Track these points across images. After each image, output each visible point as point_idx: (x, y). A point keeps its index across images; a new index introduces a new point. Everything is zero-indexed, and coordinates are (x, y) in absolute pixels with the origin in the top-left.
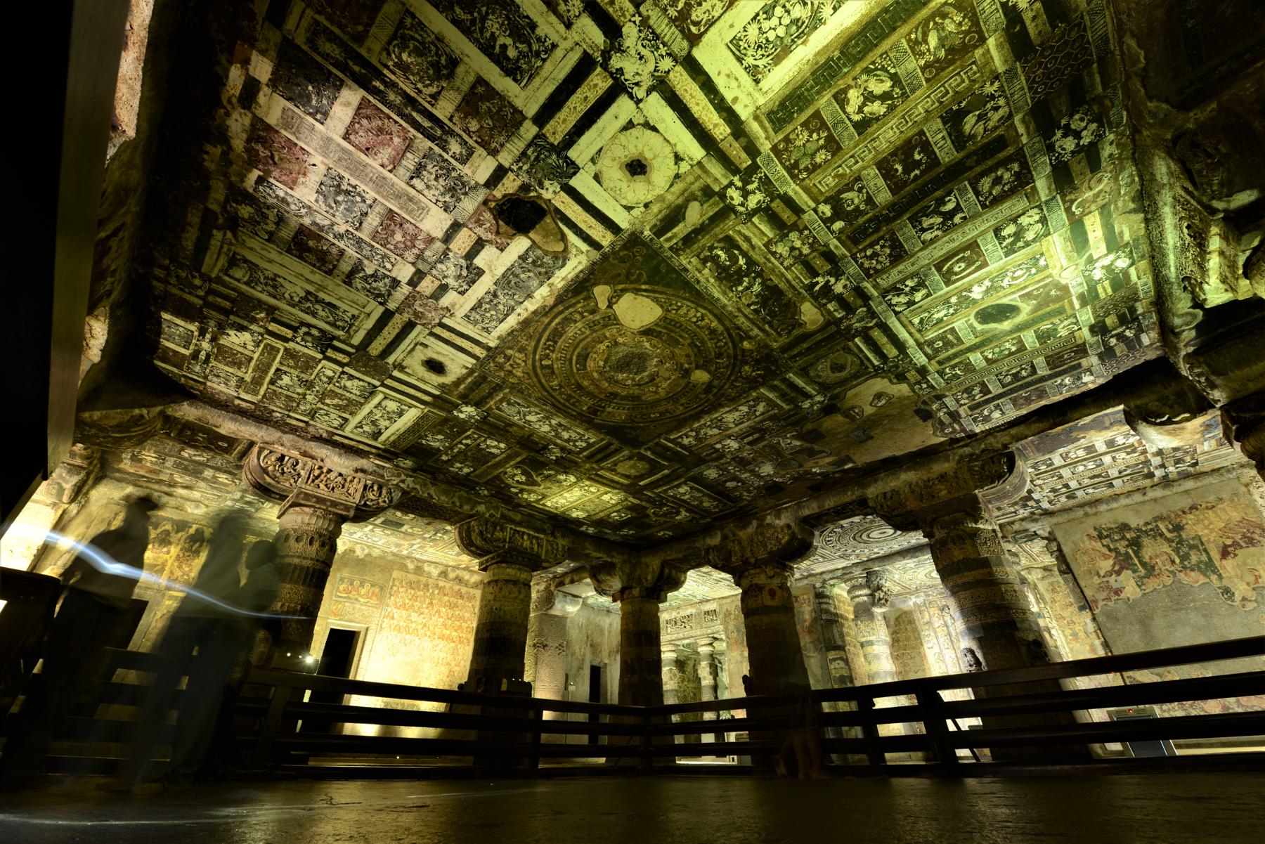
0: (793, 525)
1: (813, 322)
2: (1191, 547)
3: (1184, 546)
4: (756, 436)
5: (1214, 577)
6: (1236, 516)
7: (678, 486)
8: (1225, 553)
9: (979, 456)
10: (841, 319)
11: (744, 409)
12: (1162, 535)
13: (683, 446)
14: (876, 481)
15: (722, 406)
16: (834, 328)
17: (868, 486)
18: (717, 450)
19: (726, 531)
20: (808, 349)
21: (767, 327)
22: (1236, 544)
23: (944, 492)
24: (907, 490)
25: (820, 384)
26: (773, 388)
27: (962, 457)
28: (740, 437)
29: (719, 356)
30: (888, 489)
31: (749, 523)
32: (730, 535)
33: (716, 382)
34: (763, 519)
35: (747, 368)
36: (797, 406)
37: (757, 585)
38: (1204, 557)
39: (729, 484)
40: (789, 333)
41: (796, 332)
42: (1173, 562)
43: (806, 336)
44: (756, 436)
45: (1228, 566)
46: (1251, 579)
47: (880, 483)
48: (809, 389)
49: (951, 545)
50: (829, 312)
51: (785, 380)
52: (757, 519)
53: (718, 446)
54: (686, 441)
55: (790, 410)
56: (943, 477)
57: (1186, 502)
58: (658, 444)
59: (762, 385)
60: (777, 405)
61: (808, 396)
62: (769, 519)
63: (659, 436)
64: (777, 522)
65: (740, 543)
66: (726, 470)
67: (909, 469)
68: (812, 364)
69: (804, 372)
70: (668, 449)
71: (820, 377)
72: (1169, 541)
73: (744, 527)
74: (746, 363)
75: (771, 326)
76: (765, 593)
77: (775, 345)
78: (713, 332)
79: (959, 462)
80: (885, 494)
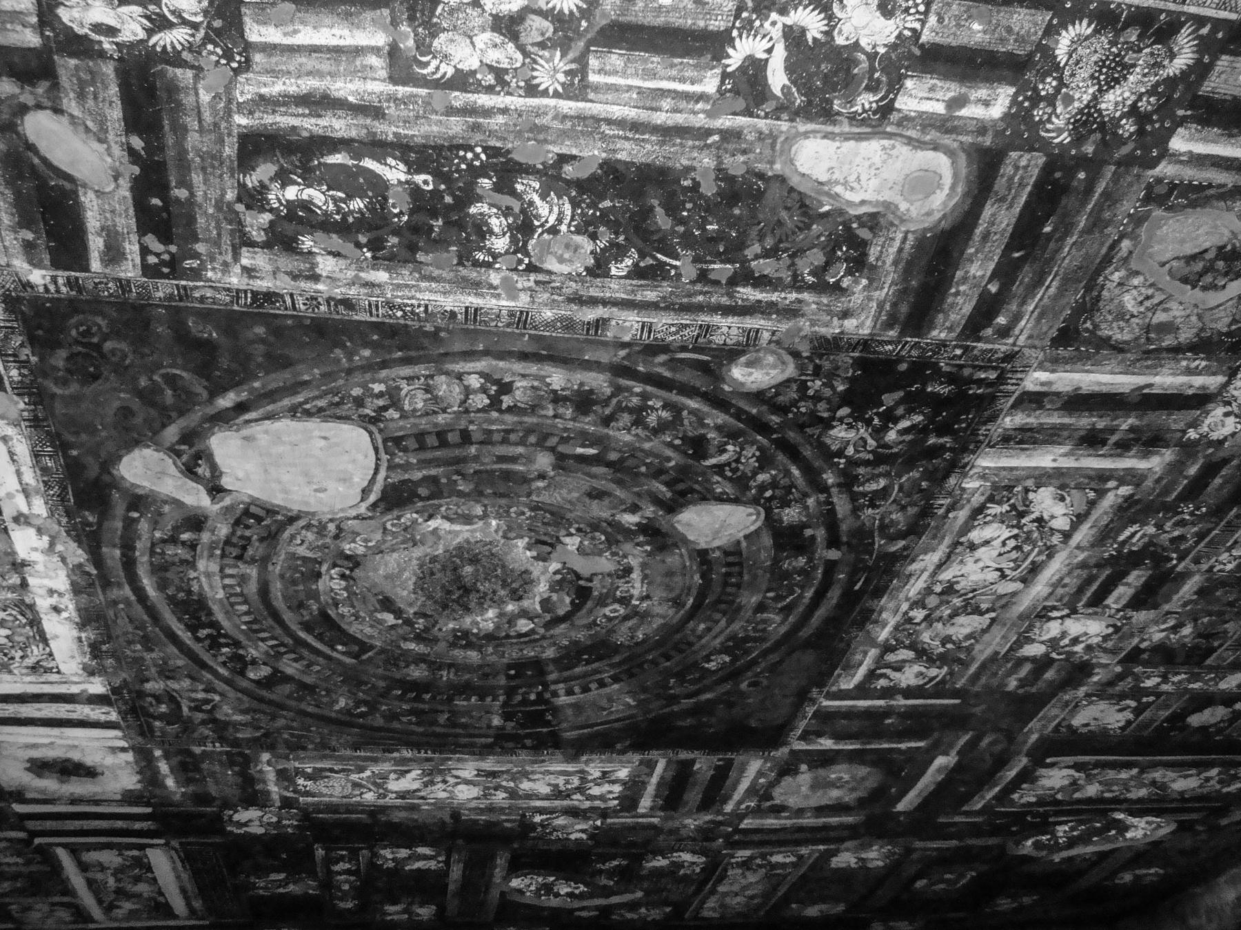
1: (921, 183)
4: (1136, 578)
7: (1026, 776)
10: (1019, 117)
11: (994, 532)
13: (909, 693)
15: (906, 556)
16: (1024, 167)
18: (1043, 663)
20: (1006, 272)
21: (748, 293)
25: (1203, 346)
26: (1025, 438)
28: (1090, 593)
29: (698, 447)
33: (791, 515)
35: (840, 433)
36: (1188, 449)
39: (1195, 720)
40: (859, 264)
41: (886, 251)
43: (939, 253)
44: (1136, 578)
48: (1166, 380)
50: (945, 125)
51: (1035, 400)
53: (1034, 650)
54: (908, 677)
55: (1175, 468)
58: (825, 717)
59: (969, 444)
60: (1103, 476)
61: (1202, 400)
63: (802, 697)
66: (1137, 692)
68: (1089, 307)
69: (1072, 340)
70: (868, 714)
71: (1168, 328)
74: (827, 424)
75: (761, 282)
77: (860, 326)
78: (584, 402)
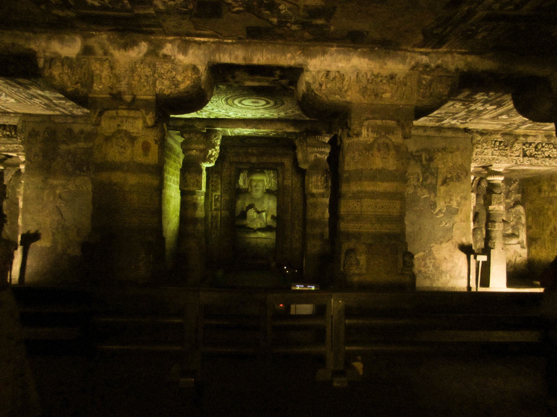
0: (202, 68)
2: (432, 174)
3: (428, 170)
5: (433, 195)
6: (460, 161)
8: (444, 182)
9: (433, 70)
12: (421, 161)
14: (324, 53)
17: (312, 55)
19: (92, 42)
22: (451, 179)
23: (388, 95)
24: (353, 77)
27: (417, 65)
30: (333, 68)
31: (134, 44)
32: (99, 52)
34: (160, 46)
37: (127, 133)
38: (434, 182)
42: (418, 180)
45: (442, 189)
46: (448, 200)
47: (328, 58)
49: (375, 152)
52: (150, 42)
56: (392, 77)
57: (442, 144)
62: (168, 49)
64: (181, 57)
65: (112, 68)
67: (363, 55)
72: (423, 166)
73: (125, 47)
76: (138, 145)
79: (413, 68)
80: (328, 72)
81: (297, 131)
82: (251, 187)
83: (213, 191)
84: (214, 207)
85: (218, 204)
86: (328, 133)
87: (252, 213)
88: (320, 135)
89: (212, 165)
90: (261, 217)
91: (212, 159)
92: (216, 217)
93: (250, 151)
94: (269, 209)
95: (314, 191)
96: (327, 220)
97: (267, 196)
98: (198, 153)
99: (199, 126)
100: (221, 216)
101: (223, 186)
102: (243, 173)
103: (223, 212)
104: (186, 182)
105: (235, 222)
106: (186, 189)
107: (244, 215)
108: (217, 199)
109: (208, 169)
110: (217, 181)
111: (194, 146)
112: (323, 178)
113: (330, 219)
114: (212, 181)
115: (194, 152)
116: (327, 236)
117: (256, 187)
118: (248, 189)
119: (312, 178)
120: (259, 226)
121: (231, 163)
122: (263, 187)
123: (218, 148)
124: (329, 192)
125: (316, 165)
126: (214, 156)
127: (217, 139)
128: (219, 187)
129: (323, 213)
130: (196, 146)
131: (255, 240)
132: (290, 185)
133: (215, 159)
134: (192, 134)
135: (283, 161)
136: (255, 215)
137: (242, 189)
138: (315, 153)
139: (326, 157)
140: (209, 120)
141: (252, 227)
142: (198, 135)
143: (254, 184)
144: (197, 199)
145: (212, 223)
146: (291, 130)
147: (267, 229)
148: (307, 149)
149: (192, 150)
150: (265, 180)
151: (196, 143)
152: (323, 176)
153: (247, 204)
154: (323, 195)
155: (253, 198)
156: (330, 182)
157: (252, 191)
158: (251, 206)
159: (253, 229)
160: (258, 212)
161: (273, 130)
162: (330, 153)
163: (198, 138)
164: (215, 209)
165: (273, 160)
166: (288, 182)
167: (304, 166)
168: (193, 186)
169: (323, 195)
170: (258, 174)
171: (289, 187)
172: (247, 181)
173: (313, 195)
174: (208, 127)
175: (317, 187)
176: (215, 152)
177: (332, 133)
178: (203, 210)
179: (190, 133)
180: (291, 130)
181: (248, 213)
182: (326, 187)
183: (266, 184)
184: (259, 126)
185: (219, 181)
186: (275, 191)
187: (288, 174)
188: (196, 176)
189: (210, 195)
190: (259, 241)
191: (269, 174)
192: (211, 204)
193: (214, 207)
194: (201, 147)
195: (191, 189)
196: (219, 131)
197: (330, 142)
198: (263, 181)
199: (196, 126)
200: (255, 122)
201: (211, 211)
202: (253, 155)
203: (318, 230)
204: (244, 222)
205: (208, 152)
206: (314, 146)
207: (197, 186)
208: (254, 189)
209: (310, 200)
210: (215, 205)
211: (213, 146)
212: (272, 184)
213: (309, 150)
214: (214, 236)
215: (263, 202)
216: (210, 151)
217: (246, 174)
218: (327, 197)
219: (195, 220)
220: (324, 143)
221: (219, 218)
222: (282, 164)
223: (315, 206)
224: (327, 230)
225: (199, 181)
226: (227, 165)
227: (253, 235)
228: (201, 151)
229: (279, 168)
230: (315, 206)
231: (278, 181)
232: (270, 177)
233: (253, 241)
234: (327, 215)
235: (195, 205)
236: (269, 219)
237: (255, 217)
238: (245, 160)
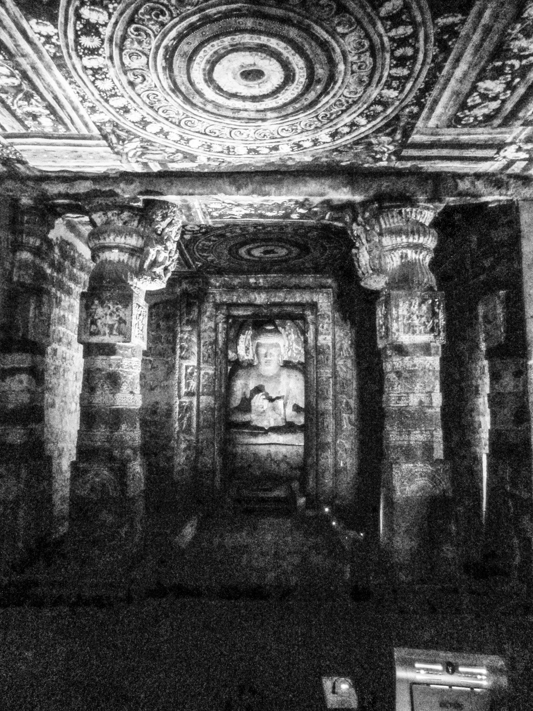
81: (358, 198)
82: (258, 358)
83: (181, 358)
84: (184, 390)
85: (193, 384)
86: (430, 200)
87: (259, 401)
88: (413, 206)
89: (159, 285)
90: (274, 409)
91: (159, 270)
92: (189, 408)
93: (252, 281)
94: (289, 392)
95: (405, 339)
96: (438, 410)
97: (285, 372)
98: (125, 257)
99: (126, 192)
100: (198, 405)
101: (202, 349)
102: (244, 334)
103: (202, 397)
104: (94, 322)
105: (228, 419)
106: (95, 340)
107: (246, 405)
108: (191, 374)
109: (149, 295)
110: (190, 340)
111: (110, 240)
112: (424, 307)
113: (443, 408)
114: (181, 339)
115: (114, 256)
116: (439, 453)
117: (266, 356)
118: (252, 360)
119: (397, 306)
120: (272, 424)
121: (217, 306)
122: (278, 356)
123: (172, 246)
124: (442, 339)
125: (404, 280)
126: (162, 263)
127: (170, 224)
128: (195, 349)
129: (429, 394)
130: (120, 240)
131: (266, 448)
132: (330, 344)
133: (166, 269)
134: (110, 214)
135: (315, 300)
136: (266, 404)
137: (243, 362)
138: (403, 247)
139: (428, 260)
140: (148, 176)
141: (260, 425)
142: (126, 215)
143: (262, 351)
144: (118, 366)
145: (181, 419)
146: (342, 195)
147: (289, 427)
148: (380, 241)
149: (110, 248)
150: (282, 346)
151: (119, 232)
152: (423, 301)
153: (252, 385)
154: (426, 349)
155: (260, 376)
156: (441, 316)
157: (259, 363)
158: (258, 390)
159: (262, 428)
160: (271, 400)
161: (301, 199)
162: (436, 250)
163: (125, 223)
164: (190, 394)
165: (298, 297)
166: (325, 340)
167: (376, 283)
168: (111, 334)
169: (426, 349)
170: (269, 335)
171: (328, 347)
172: (250, 348)
173: (401, 350)
174: (147, 192)
175: (410, 328)
176: (166, 256)
177: (440, 201)
178: (137, 390)
179: (104, 209)
180: (342, 195)
181: (252, 401)
182: (432, 330)
183: (282, 351)
184: (267, 188)
185: (195, 339)
186: (299, 363)
187: (326, 325)
188: (117, 310)
189: (177, 366)
190: (273, 449)
191: (287, 336)
192: (179, 383)
193: (184, 390)
194: (134, 241)
195: (107, 339)
196: (174, 205)
197: (435, 224)
198: (277, 346)
199: (118, 191)
200: (257, 178)
201: (180, 397)
202: (257, 288)
203: (417, 437)
204: (247, 417)
205: (148, 253)
206: (398, 232)
207: (120, 333)
208: (263, 360)
209: (394, 363)
210: (188, 385)
211: (161, 239)
212: (292, 351)
213: (387, 241)
214: (183, 446)
215: (279, 382)
216: (152, 253)
217: (249, 337)
218: (437, 353)
219: (117, 417)
220: (422, 225)
221: (195, 409)
222: (313, 306)
223: (409, 376)
224: (439, 434)
225: (125, 322)
226: (209, 309)
227: (261, 440)
228: (133, 252)
229: (308, 312)
230: (409, 376)
231: (306, 341)
232: (288, 339)
233: (263, 451)
234: (438, 399)
235: (114, 380)
236: (289, 411)
237: (265, 408)
238: (244, 300)
